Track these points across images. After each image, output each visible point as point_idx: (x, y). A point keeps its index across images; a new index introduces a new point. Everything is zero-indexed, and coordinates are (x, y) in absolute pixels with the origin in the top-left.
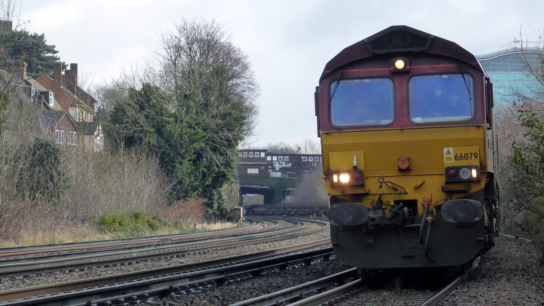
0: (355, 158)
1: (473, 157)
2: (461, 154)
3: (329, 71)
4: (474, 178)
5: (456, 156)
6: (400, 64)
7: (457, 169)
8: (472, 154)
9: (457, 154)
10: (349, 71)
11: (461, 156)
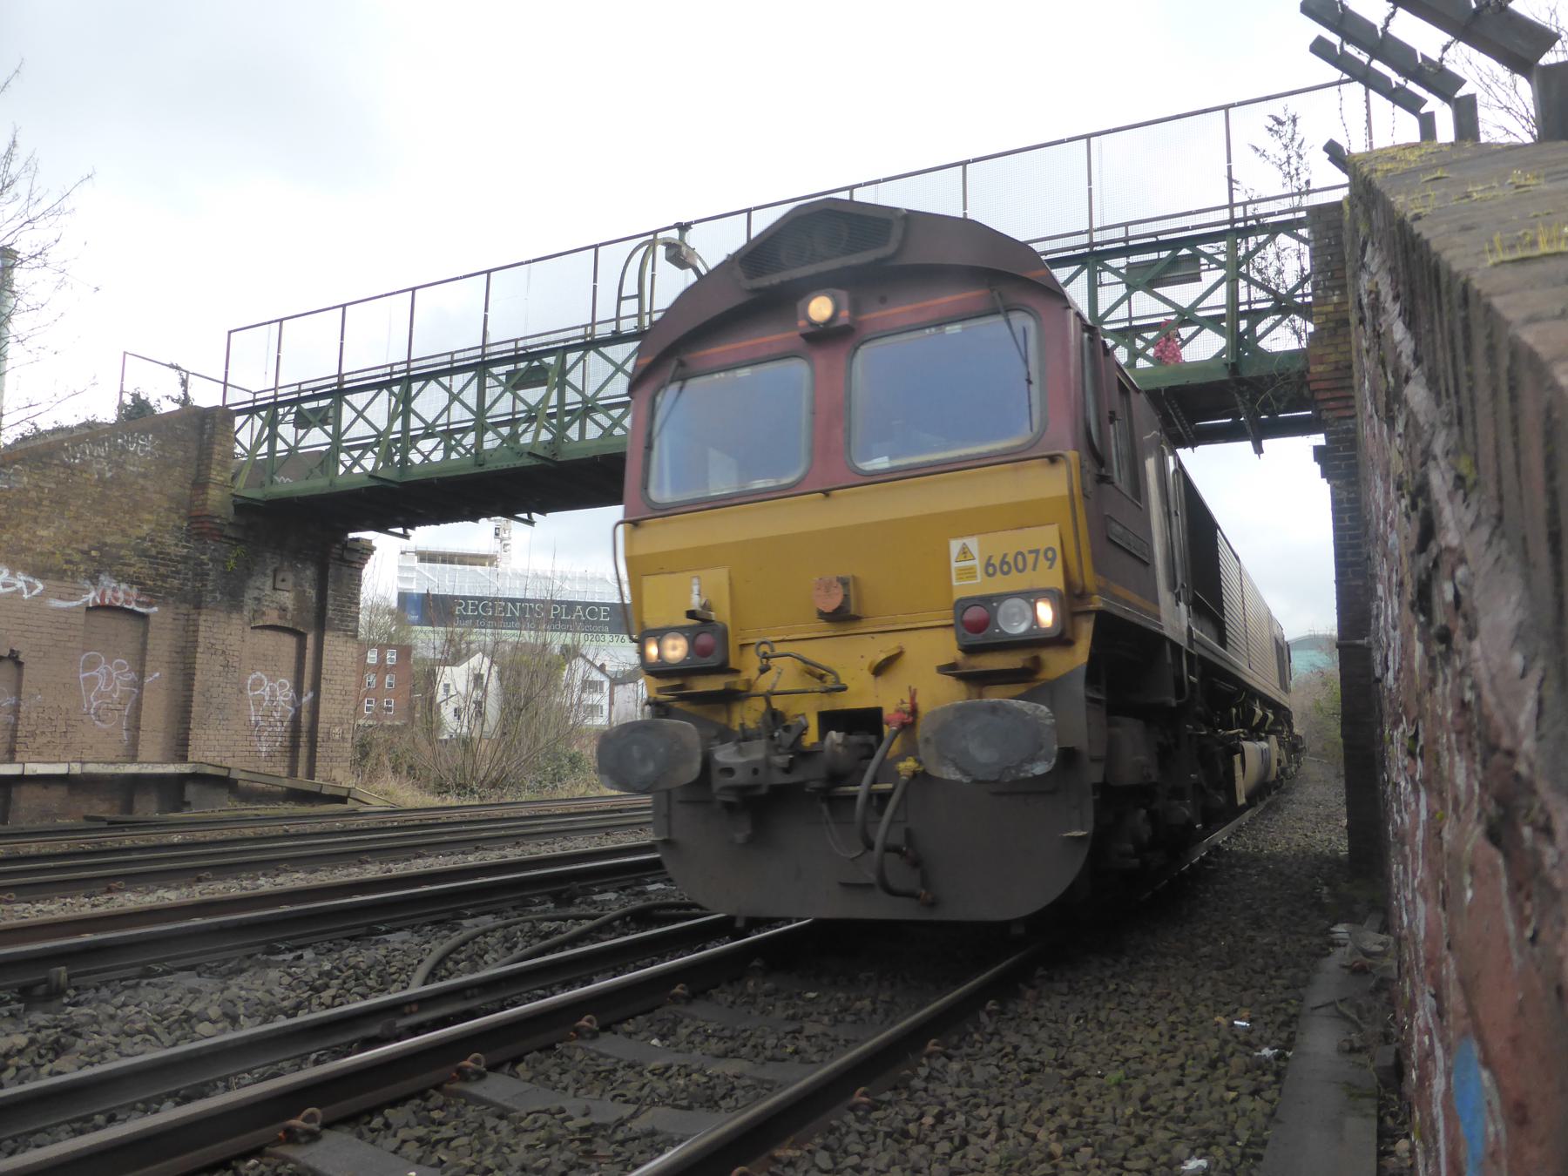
0: (695, 588)
1: (1043, 563)
2: (1005, 556)
3: (647, 360)
4: (1047, 629)
5: (988, 564)
6: (820, 308)
7: (987, 601)
8: (1037, 552)
9: (990, 558)
10: (702, 353)
11: (1003, 562)
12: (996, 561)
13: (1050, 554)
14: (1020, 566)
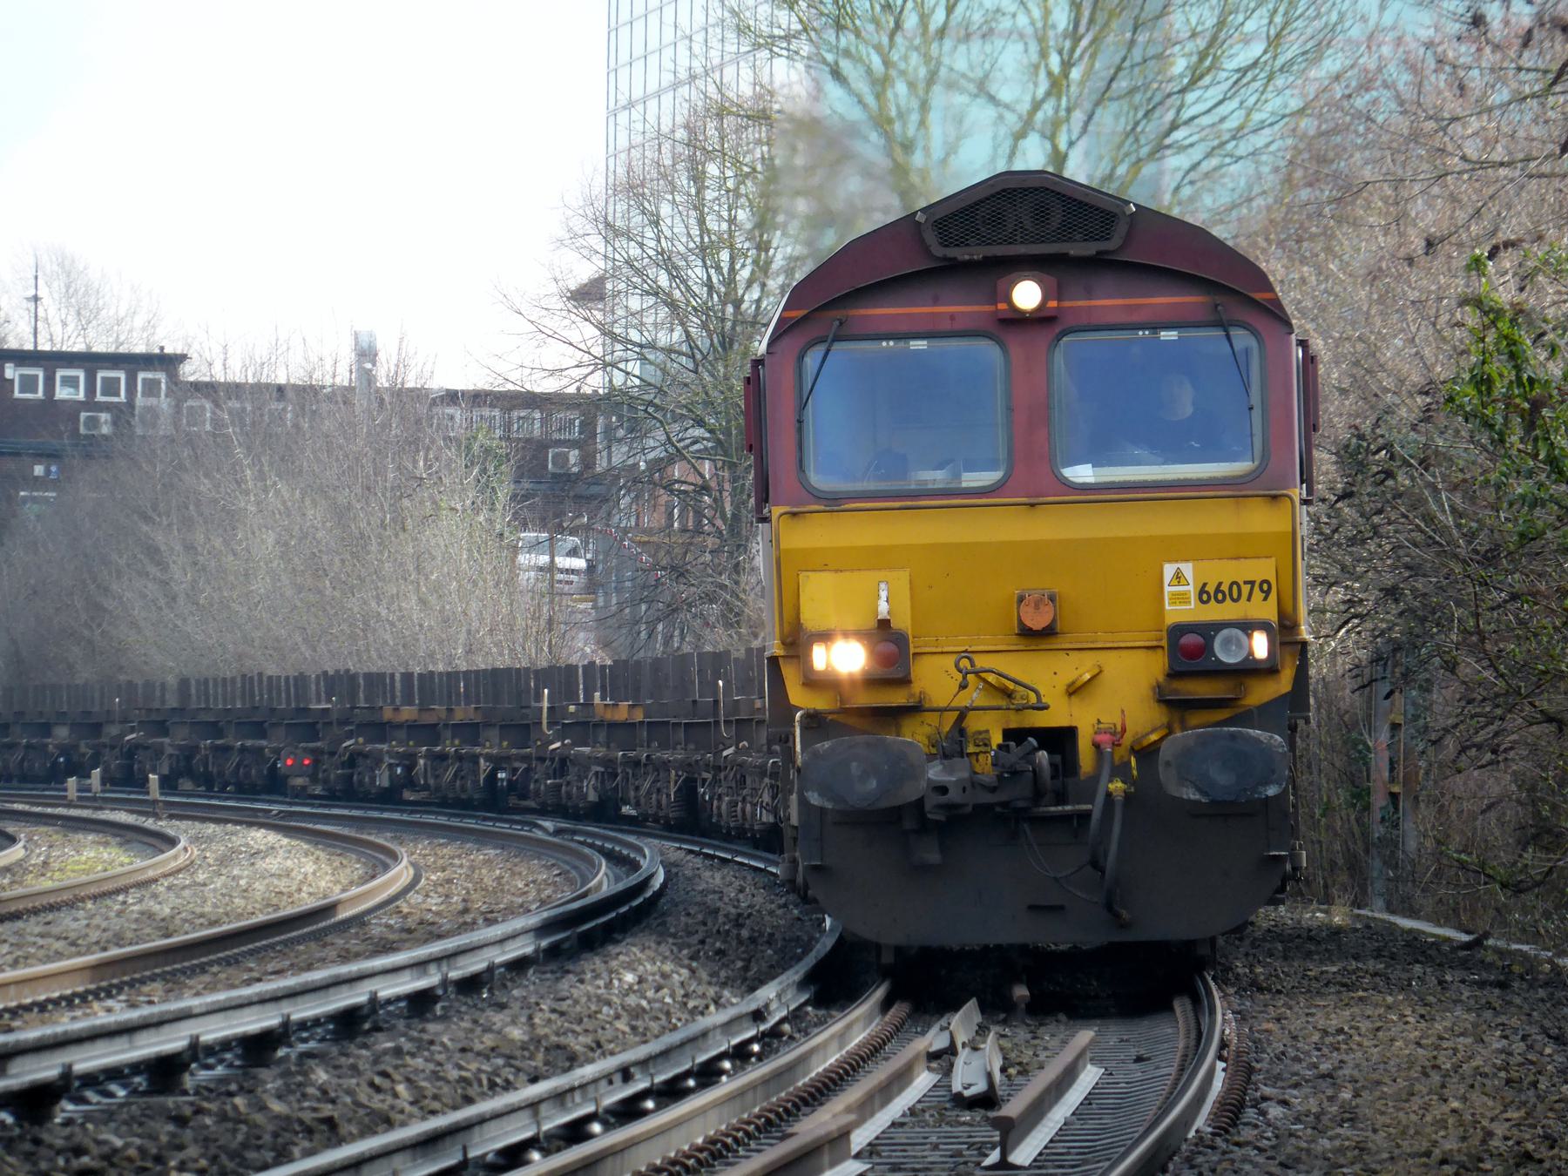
0: (884, 595)
2: (1220, 584)
4: (1261, 661)
5: (1202, 591)
6: (1027, 295)
7: (1208, 630)
8: (1252, 583)
9: (1205, 585)
10: (863, 312)
11: (1218, 590)
12: (1211, 589)
13: (1265, 587)
14: (1235, 596)
